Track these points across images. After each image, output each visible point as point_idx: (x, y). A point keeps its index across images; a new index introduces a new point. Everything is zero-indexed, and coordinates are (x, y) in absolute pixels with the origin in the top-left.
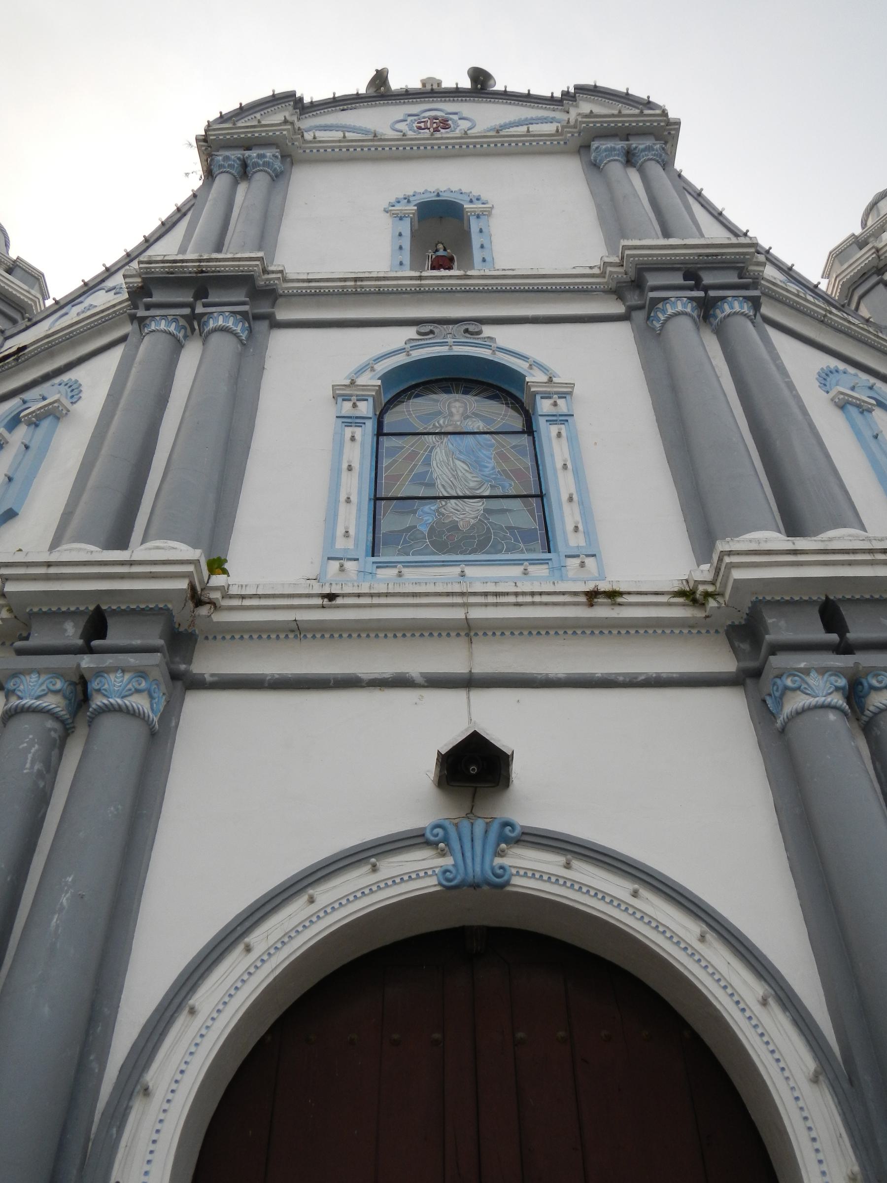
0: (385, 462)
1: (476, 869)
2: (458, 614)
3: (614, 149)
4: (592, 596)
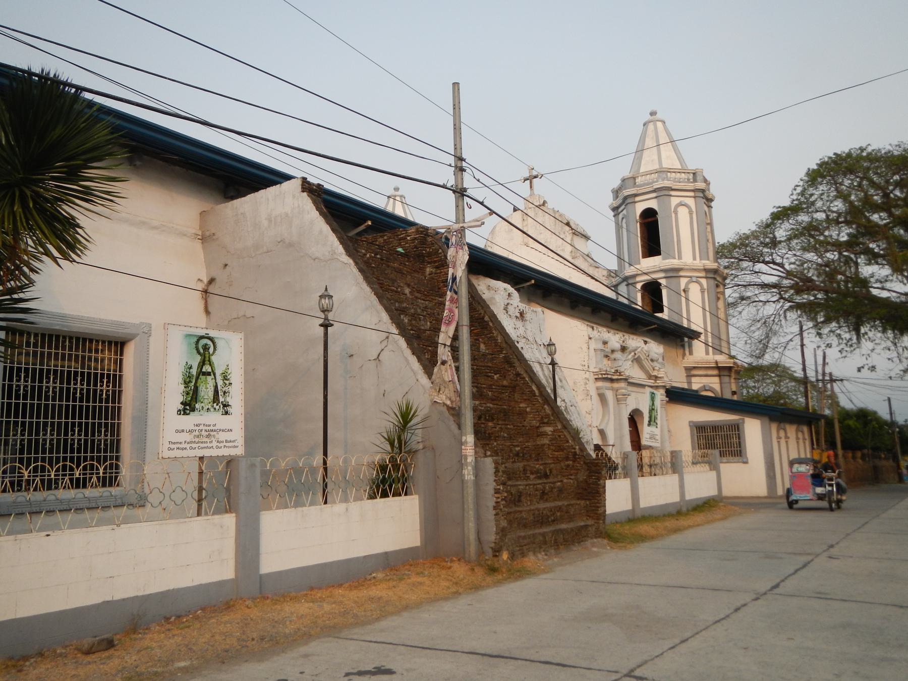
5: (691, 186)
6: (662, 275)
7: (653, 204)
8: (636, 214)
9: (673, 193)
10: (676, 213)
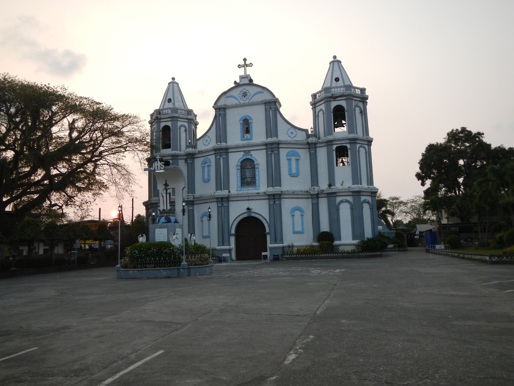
0: (242, 173)
1: (249, 215)
2: (247, 195)
4: (257, 193)
5: (185, 117)
6: (170, 158)
7: (169, 124)
9: (179, 119)
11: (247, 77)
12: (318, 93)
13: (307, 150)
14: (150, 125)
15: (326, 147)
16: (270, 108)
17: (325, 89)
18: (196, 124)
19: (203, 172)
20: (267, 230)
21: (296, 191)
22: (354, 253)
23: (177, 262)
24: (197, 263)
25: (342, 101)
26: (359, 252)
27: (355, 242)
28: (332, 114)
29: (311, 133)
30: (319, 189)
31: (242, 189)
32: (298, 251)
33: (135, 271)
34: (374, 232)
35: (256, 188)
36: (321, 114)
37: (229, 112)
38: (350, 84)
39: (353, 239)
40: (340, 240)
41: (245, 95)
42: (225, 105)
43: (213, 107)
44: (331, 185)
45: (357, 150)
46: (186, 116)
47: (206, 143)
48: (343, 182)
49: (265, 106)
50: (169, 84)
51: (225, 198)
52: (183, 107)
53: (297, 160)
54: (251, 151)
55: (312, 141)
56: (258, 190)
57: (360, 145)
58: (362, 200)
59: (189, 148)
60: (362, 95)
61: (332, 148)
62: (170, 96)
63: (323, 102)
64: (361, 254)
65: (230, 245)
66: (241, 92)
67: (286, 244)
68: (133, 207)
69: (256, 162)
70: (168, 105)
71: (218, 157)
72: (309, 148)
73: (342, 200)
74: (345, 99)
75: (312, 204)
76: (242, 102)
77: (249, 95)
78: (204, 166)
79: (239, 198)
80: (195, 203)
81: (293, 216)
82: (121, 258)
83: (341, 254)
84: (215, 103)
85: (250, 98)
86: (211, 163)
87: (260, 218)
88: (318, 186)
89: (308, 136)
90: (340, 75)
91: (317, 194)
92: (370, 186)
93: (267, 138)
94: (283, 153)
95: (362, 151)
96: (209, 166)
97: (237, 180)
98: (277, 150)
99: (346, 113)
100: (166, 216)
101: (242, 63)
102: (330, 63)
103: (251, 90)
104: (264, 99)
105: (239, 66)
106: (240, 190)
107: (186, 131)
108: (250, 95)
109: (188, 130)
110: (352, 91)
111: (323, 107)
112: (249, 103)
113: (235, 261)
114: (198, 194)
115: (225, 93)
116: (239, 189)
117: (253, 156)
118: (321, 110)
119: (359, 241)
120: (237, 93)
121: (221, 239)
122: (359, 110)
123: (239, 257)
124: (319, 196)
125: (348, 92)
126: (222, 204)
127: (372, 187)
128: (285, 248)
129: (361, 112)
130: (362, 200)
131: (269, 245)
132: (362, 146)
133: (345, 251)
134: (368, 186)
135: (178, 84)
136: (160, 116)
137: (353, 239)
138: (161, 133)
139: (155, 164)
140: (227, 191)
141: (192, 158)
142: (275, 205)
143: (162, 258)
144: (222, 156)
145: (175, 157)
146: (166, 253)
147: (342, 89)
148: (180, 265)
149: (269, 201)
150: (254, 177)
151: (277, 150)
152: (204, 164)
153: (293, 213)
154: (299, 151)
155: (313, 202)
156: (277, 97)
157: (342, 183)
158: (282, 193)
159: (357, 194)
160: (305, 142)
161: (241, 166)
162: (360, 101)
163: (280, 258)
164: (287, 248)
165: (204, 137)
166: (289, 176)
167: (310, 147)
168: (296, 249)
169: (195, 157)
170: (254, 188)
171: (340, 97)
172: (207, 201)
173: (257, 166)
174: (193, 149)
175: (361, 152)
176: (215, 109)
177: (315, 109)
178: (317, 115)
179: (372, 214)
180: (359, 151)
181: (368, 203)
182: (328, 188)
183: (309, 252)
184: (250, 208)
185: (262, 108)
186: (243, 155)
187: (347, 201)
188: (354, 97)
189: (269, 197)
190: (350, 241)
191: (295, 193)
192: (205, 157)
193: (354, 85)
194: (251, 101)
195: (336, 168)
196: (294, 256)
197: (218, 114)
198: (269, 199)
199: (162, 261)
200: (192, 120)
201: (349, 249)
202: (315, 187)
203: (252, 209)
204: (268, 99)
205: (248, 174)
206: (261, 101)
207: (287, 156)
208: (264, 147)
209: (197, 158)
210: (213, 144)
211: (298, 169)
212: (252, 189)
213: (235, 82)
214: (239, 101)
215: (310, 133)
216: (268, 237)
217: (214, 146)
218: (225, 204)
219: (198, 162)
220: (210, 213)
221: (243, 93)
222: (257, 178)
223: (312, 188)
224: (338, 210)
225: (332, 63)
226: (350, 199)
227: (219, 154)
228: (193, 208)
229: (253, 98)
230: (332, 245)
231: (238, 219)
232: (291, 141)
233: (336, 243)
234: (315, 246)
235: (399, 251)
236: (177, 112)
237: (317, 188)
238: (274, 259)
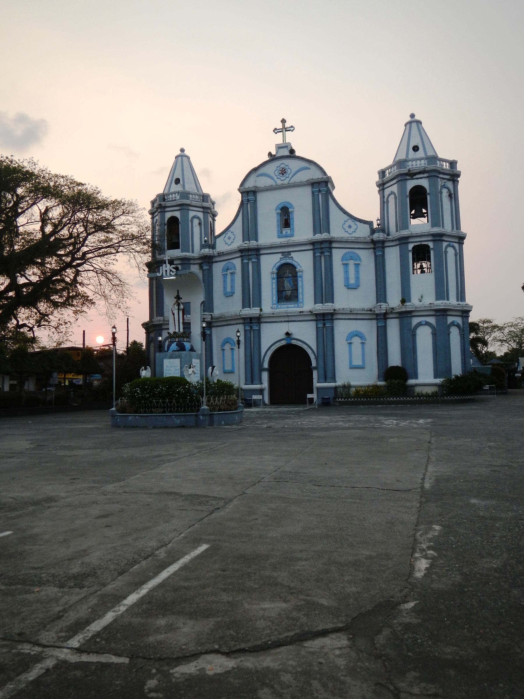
2: (286, 315)
3: (316, 191)
4: (300, 312)
5: (199, 204)
7: (177, 214)
8: (165, 219)
9: (191, 208)
10: (192, 222)
11: (287, 147)
12: (388, 168)
13: (372, 250)
14: (150, 216)
15: (398, 247)
16: (320, 191)
17: (399, 163)
18: (214, 215)
19: (225, 282)
20: (314, 364)
21: (354, 309)
22: (437, 396)
23: (196, 406)
24: (222, 407)
25: (423, 179)
26: (443, 395)
27: (438, 381)
28: (408, 199)
29: (378, 227)
30: (387, 306)
31: (279, 306)
32: (357, 392)
33: (137, 417)
34: (465, 367)
35: (298, 305)
36: (392, 199)
37: (261, 198)
38: (434, 154)
39: (436, 377)
40: (416, 377)
41: (283, 172)
42: (256, 187)
43: (239, 190)
44: (405, 300)
45: (442, 249)
46: (200, 203)
47: (229, 242)
48: (422, 297)
49: (313, 187)
50: (177, 157)
51: (254, 318)
52: (196, 191)
53: (357, 265)
54: (291, 253)
55: (379, 238)
56: (301, 307)
57: (448, 243)
58: (449, 322)
59: (205, 248)
60: (452, 170)
61: (408, 247)
62: (178, 175)
63: (395, 181)
64: (447, 398)
65: (261, 383)
66: (278, 168)
67: (339, 382)
68: (128, 330)
69: (299, 268)
70: (175, 188)
71: (245, 261)
72: (374, 249)
73: (421, 322)
74: (428, 177)
75: (378, 327)
76: (279, 182)
77: (289, 173)
78: (227, 274)
79: (274, 319)
80: (214, 324)
81: (350, 344)
82: (117, 399)
83: (418, 398)
84: (242, 185)
85: (290, 176)
86: (235, 269)
87: (304, 347)
88: (385, 302)
89: (373, 231)
90: (420, 142)
91: (385, 314)
92: (461, 301)
93: (315, 233)
94: (337, 255)
95: (450, 251)
96: (232, 274)
97: (272, 292)
98: (329, 250)
99: (428, 197)
100: (178, 341)
101: (280, 126)
102: (406, 125)
103: (293, 165)
104: (311, 178)
105: (276, 131)
106: (276, 307)
107: (200, 224)
108: (291, 171)
109: (203, 223)
110: (438, 166)
111: (395, 188)
112: (289, 183)
113: (269, 405)
114: (217, 312)
115: (255, 170)
116: (275, 306)
117: (295, 259)
118: (392, 193)
119: (444, 379)
120: (272, 168)
121: (249, 376)
122: (447, 192)
123: (275, 400)
124: (388, 316)
125: (431, 167)
126: (251, 327)
127: (464, 303)
128: (339, 390)
129: (450, 196)
130: (449, 322)
131: (316, 384)
132: (451, 245)
133: (422, 394)
134: (458, 303)
135: (188, 158)
136: (164, 203)
137: (436, 377)
138: (166, 227)
139: (162, 269)
140: (259, 309)
141: (209, 263)
142: (325, 329)
143: (174, 401)
144: (251, 259)
145: (186, 261)
146: (179, 393)
147: (423, 161)
148: (198, 410)
149: (316, 323)
150: (295, 289)
151: (329, 250)
152: (226, 270)
153: (351, 340)
154: (359, 252)
155: (379, 325)
156: (329, 175)
157: (420, 298)
158: (335, 312)
159: (443, 314)
160: (368, 240)
161: (278, 274)
162: (449, 180)
163: (332, 402)
164: (342, 389)
165: (226, 233)
166: (345, 288)
167: (376, 246)
168: (353, 390)
169: (214, 260)
170: (296, 305)
171: (420, 174)
172: (229, 323)
173: (301, 273)
174: (211, 250)
175: (448, 254)
176: (242, 193)
177: (383, 192)
178: (385, 200)
179: (462, 342)
180: (446, 252)
181: (458, 326)
182: (401, 305)
183: (372, 395)
184: (290, 333)
185: (307, 191)
186: (281, 258)
187: (427, 324)
188: (440, 173)
189: (316, 318)
190: (431, 380)
191: (353, 312)
192: (228, 261)
193: (440, 156)
194: (292, 181)
195: (412, 277)
196: (351, 399)
197: (245, 199)
198: (316, 320)
199: (174, 405)
200: (209, 208)
201: (429, 390)
202: (382, 304)
203: (293, 333)
204: (317, 177)
205: (287, 285)
206: (307, 181)
207: (343, 259)
208: (311, 247)
209: (216, 262)
210: (238, 242)
211: (357, 278)
212: (293, 305)
213: (270, 154)
214: (275, 182)
215: (375, 226)
216: (315, 374)
217: (241, 245)
218: (255, 328)
219: (218, 269)
220: (238, 338)
221: (281, 169)
222: (300, 290)
223: (379, 304)
224: (414, 336)
225: (409, 124)
226: (432, 320)
227: (247, 257)
228: (211, 332)
229: (294, 177)
230: (405, 384)
231: (274, 346)
232: (349, 238)
233: (411, 382)
234: (381, 386)
235: (497, 394)
236: (188, 198)
237: (384, 306)
238: (323, 403)
